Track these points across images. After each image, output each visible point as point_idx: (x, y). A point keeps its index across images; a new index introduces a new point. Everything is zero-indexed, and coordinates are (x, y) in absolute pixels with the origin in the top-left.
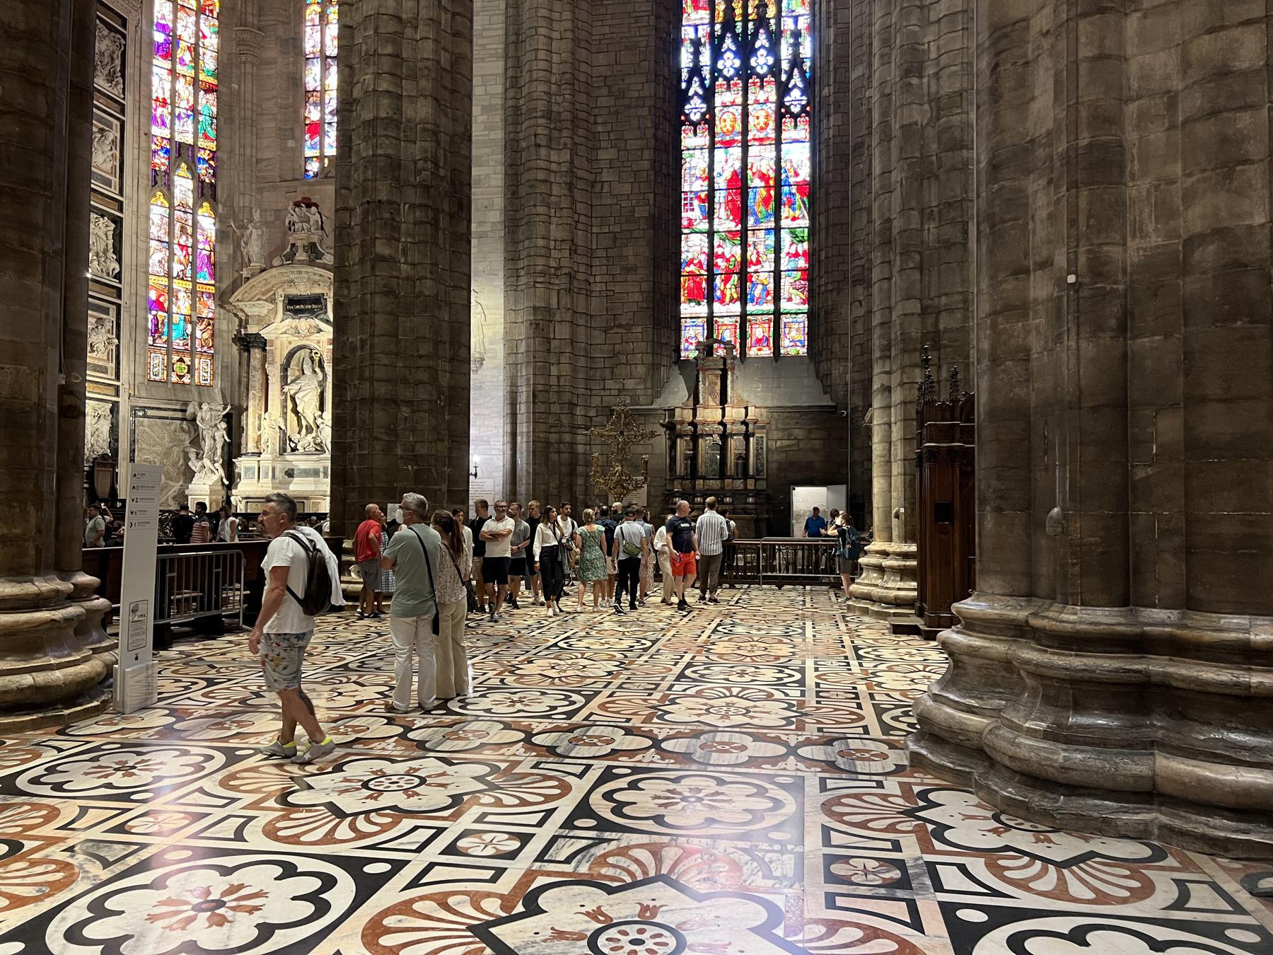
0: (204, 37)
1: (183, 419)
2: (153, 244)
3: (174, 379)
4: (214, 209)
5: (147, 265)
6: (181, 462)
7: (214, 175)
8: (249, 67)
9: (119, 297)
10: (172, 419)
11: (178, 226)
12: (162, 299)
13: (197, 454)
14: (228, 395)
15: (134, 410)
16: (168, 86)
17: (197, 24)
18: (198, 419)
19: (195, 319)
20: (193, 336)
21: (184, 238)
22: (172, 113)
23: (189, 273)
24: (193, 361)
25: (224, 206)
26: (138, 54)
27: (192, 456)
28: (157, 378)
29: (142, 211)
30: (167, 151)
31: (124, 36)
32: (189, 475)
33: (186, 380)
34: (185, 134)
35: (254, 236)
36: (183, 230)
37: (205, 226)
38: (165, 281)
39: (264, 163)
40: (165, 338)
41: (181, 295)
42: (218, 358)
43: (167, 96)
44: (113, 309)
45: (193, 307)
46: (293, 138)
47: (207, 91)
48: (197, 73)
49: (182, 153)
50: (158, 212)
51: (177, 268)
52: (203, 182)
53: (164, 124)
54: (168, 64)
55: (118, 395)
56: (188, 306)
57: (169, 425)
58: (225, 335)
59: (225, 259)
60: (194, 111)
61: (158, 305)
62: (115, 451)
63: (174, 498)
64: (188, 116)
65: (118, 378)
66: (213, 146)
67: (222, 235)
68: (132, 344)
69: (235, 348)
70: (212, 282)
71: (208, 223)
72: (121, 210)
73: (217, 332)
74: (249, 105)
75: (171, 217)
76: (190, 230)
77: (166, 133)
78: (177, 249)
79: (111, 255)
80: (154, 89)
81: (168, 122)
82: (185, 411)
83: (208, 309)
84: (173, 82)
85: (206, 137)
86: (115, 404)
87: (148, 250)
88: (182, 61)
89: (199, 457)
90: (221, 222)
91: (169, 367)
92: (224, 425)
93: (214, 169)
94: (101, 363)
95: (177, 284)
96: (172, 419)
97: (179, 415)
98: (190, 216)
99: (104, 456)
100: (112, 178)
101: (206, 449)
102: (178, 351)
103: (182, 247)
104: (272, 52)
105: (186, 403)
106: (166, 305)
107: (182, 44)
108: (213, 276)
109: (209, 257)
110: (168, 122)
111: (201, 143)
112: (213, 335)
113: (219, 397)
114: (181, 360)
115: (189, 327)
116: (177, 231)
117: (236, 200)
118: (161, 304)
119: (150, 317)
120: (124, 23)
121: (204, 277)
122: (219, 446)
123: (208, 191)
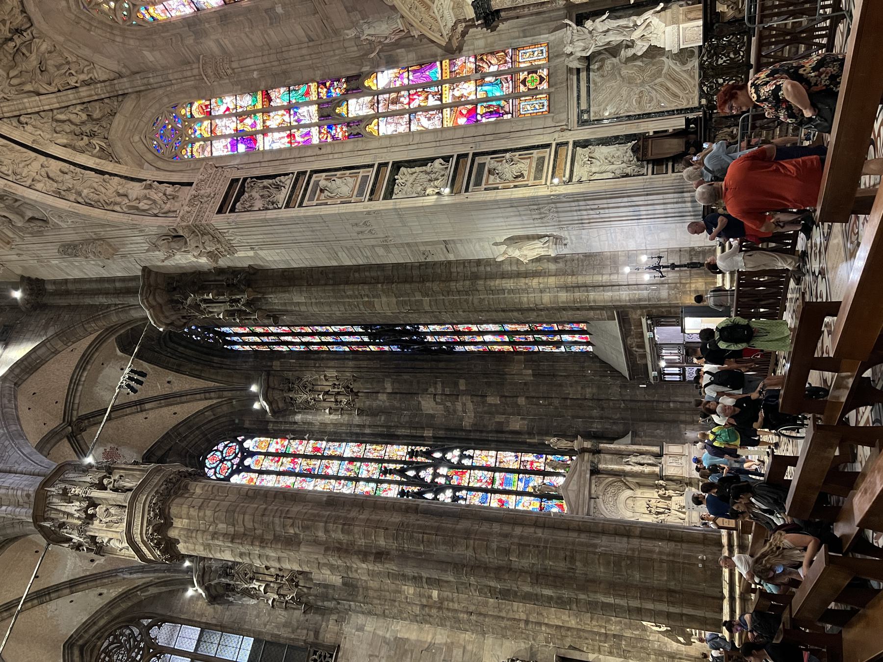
0: (228, 109)
1: (588, 70)
2: (414, 128)
3: (545, 85)
4: (368, 75)
5: (435, 131)
6: (639, 63)
7: (339, 80)
8: (235, 65)
9: (467, 155)
10: (588, 81)
11: (392, 107)
12: (464, 112)
13: (628, 47)
14: (553, 25)
15: (582, 123)
16: (277, 135)
17: (220, 117)
18: (584, 54)
19: (478, 76)
20: (495, 74)
21: (402, 99)
22: (298, 128)
23: (434, 89)
24: (523, 70)
25: (362, 65)
26: (258, 165)
27: (630, 52)
28: (546, 103)
29: (386, 143)
30: (330, 127)
31: (245, 179)
32: (654, 52)
33: (544, 73)
34: (309, 114)
35: (372, 31)
36: (395, 102)
37: (387, 81)
38: (447, 111)
39: (310, 33)
40: (502, 103)
41: (457, 93)
42: (515, 43)
43: (284, 134)
44: (479, 160)
45: (467, 79)
46: (273, 9)
47: (270, 100)
48: (258, 111)
49: (328, 113)
50: (385, 128)
51: (432, 102)
52: (347, 90)
53: (308, 134)
54: (260, 137)
55: (567, 143)
56: (466, 85)
57: (595, 84)
58: (490, 40)
59: (412, 56)
60: (289, 108)
61: (472, 114)
62: (629, 138)
63: (684, 64)
64: (295, 113)
65: (548, 146)
66: (313, 86)
67: (391, 63)
68: (512, 135)
69: (502, 26)
70: (438, 64)
71: (384, 79)
72: (386, 164)
73: (488, 50)
74: (265, 59)
75: (386, 115)
76: (393, 95)
77: (314, 131)
78: (414, 105)
79: (428, 168)
80: (283, 146)
81: (305, 131)
82: (578, 70)
83: (466, 63)
84: (272, 130)
85: (307, 93)
86: (576, 144)
87: (420, 133)
88: (254, 125)
89: (631, 45)
90: (378, 66)
91: (533, 93)
92: (589, 24)
93: (333, 82)
94: (534, 165)
95: (448, 99)
96: (588, 81)
97: (583, 75)
98: (381, 97)
99: (635, 150)
100: (361, 175)
101: (620, 38)
102: (514, 88)
103: (412, 100)
104: (210, 44)
105: (570, 70)
106: (470, 107)
107: (240, 127)
108: (432, 65)
109: (415, 72)
110: (305, 131)
111: (314, 97)
112: (492, 53)
113: (559, 34)
114: (524, 82)
115: (487, 79)
116: (397, 107)
117: (353, 55)
118: (469, 111)
119: (484, 120)
120: (234, 181)
121: (435, 73)
122: (614, 23)
123: (354, 84)
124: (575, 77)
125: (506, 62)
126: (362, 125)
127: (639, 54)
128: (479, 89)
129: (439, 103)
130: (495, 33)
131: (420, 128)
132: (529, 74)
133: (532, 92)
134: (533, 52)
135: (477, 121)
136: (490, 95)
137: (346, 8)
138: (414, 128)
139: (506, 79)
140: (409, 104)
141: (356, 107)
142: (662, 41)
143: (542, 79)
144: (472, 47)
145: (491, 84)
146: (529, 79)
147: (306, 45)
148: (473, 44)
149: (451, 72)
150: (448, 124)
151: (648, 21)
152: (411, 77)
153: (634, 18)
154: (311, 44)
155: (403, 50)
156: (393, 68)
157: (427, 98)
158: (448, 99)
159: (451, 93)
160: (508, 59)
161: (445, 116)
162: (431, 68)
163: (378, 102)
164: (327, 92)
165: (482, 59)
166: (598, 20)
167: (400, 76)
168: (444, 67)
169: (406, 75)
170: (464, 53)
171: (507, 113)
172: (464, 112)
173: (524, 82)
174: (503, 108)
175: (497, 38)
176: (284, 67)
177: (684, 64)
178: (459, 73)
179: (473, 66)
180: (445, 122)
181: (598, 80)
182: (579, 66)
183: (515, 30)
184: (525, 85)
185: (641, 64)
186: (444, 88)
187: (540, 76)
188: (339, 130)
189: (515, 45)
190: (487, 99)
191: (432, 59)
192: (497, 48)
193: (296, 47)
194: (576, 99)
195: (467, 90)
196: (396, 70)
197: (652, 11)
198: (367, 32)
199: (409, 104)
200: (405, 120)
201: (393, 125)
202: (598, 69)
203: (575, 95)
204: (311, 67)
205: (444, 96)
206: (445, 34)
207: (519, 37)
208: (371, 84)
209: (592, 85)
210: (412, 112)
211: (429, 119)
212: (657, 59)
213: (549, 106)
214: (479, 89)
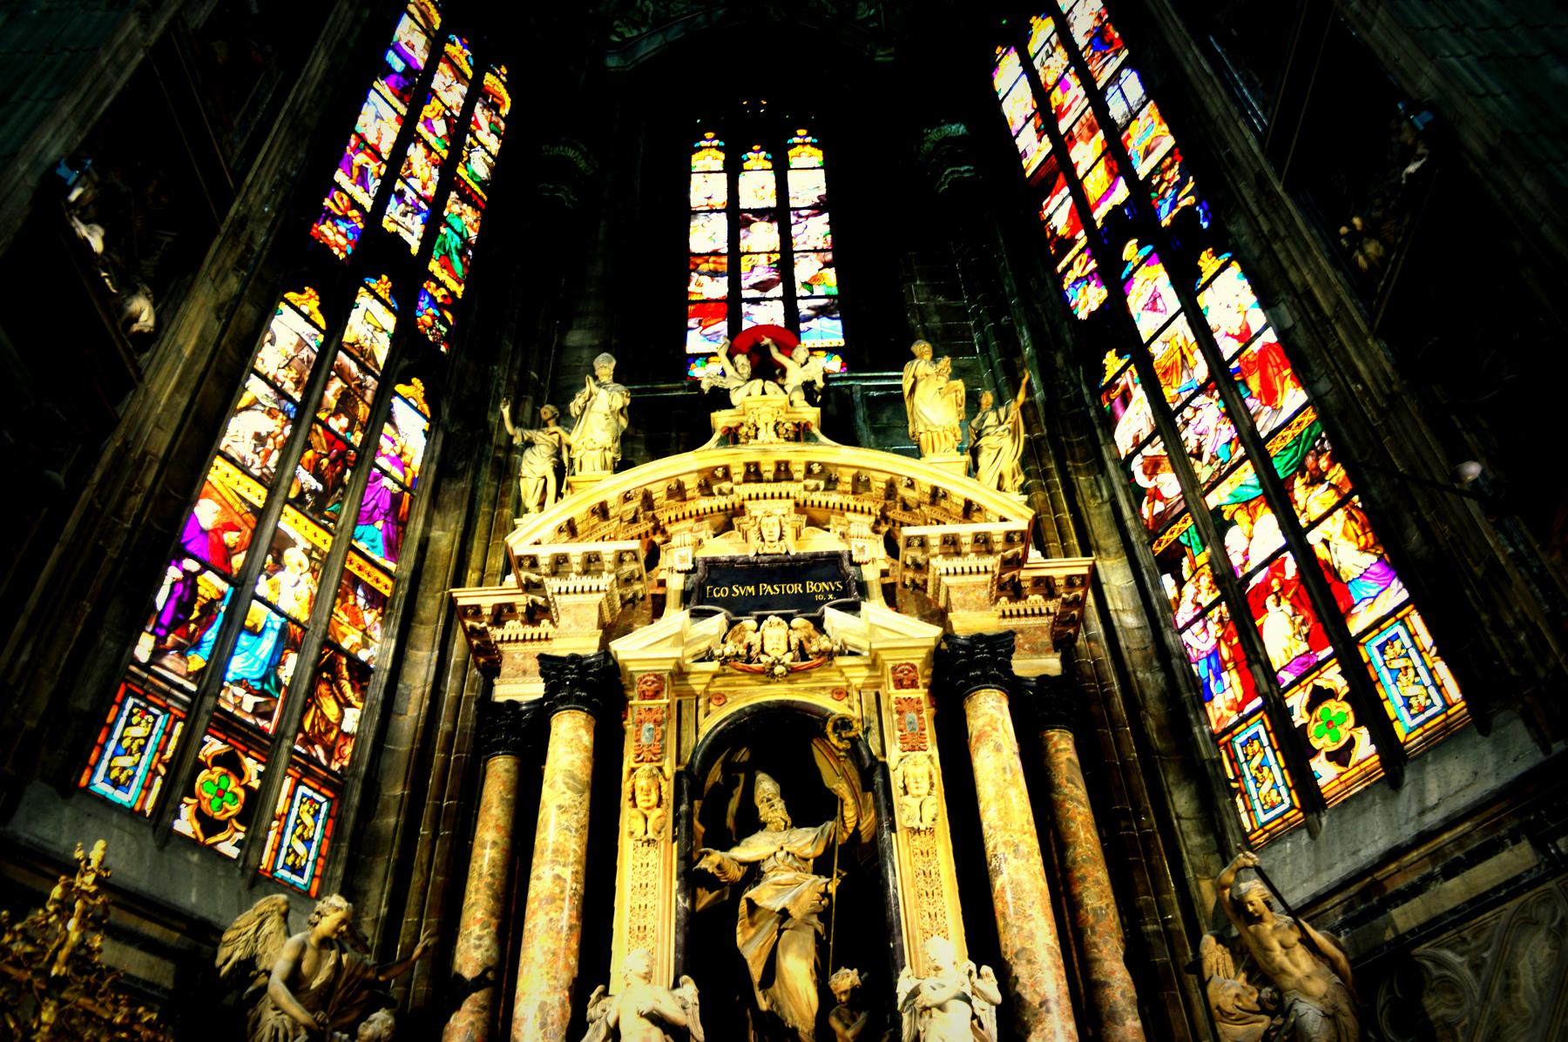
2: (255, 388)
11: (336, 385)
12: (230, 538)
28: (119, 796)
38: (257, 495)
40: (197, 661)
76: (363, 411)
102: (227, 725)
106: (237, 561)
114: (230, 763)
128: (277, 621)
132: (247, 788)
133: (189, 764)
134: (308, 842)
136: (244, 640)
139: (268, 716)
141: (371, 322)
143: (211, 825)
145: (276, 662)
146: (232, 784)
157: (317, 474)
158: (292, 523)
163: (363, 368)
164: (433, 298)
167: (397, 460)
169: (400, 477)
174: (182, 650)
184: (218, 760)
186: (322, 534)
188: (342, 241)
190: (235, 624)
211: (260, 439)
214: (277, 621)
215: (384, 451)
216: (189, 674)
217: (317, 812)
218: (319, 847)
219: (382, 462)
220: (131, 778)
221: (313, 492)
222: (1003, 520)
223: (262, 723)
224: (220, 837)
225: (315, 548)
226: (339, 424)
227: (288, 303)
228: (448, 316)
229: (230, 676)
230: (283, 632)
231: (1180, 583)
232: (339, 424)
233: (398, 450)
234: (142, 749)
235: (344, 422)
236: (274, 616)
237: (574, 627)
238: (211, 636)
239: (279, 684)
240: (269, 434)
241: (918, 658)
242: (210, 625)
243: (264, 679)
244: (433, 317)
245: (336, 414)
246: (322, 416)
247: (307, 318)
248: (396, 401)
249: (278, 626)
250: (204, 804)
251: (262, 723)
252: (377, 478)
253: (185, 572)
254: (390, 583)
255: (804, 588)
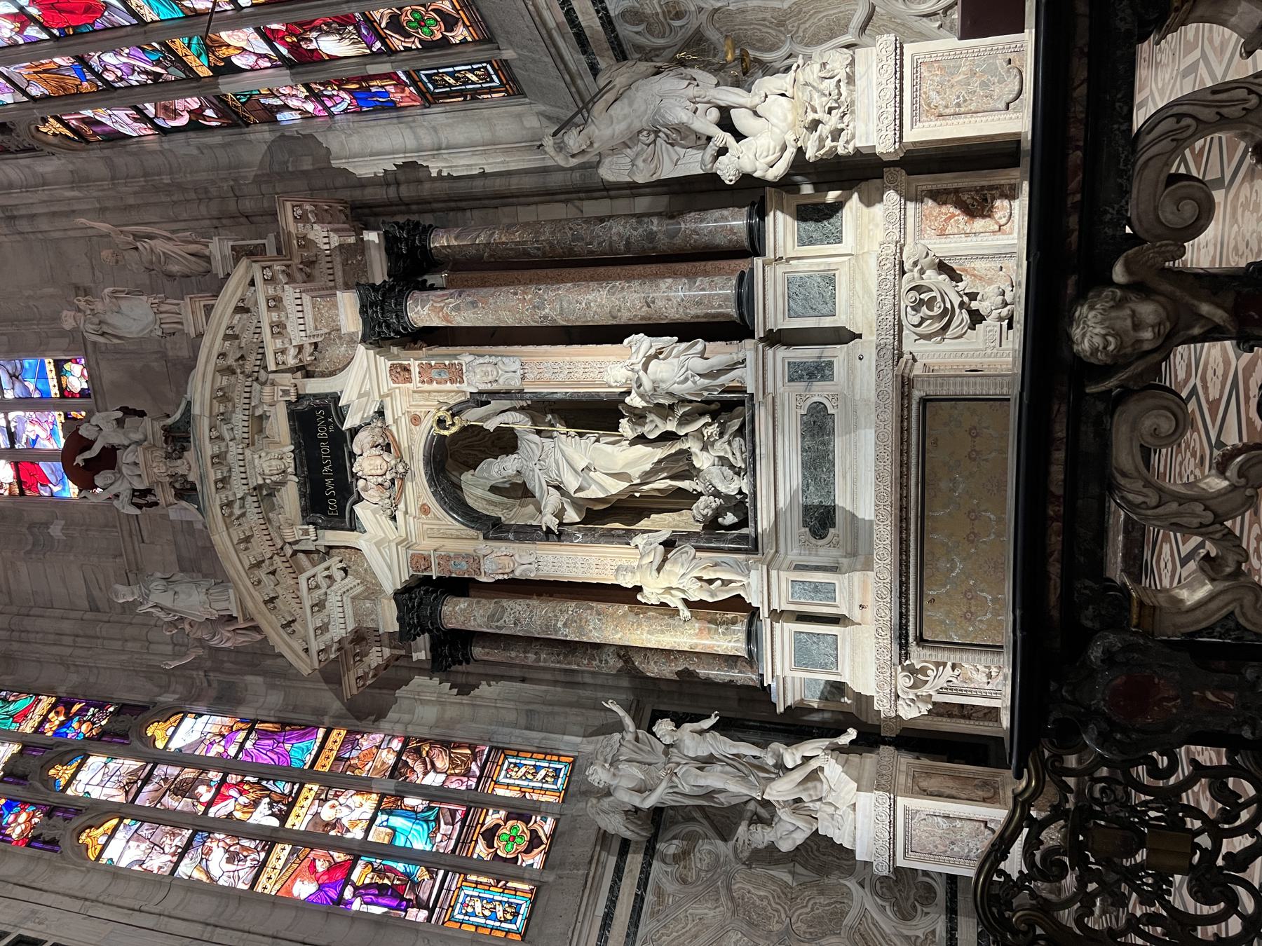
1: (650, 852)
2: (186, 869)
3: (536, 860)
6: (783, 875)
7: (101, 706)
10: (643, 883)
11: (170, 802)
12: (321, 866)
13: (756, 820)
18: (636, 800)
20: (434, 795)
24: (499, 803)
25: (166, 689)
27: (762, 836)
28: (524, 910)
29: (96, 885)
32: (824, 855)
35: (166, 600)
37: (196, 736)
38: (282, 852)
39: (96, 593)
40: (420, 873)
41: (327, 814)
42: (505, 736)
45: (362, 786)
50: (123, 849)
51: (262, 817)
52: (104, 732)
57: (660, 893)
58: (451, 712)
59: (275, 699)
63: (905, 915)
66: (46, 702)
67: (223, 702)
70: (321, 732)
71: (189, 733)
73: (438, 733)
75: (142, 816)
76: (189, 773)
82: (625, 845)
83: (378, 751)
89: (765, 814)
90: (197, 699)
91: (503, 870)
92: (664, 727)
93: (89, 706)
95: (299, 821)
96: (643, 883)
97: (635, 861)
102: (463, 841)
103: (219, 796)
105: (604, 838)
106: (339, 857)
108: (306, 730)
109: (264, 734)
114: (490, 835)
115: (410, 801)
119: (357, 905)
121: (301, 752)
122: (725, 746)
124: (612, 861)
125: (467, 773)
126: (77, 822)
127: (785, 846)
128: (381, 818)
129: (275, 822)
130: (465, 700)
131: (197, 875)
132: (507, 819)
133: (499, 866)
134: (537, 769)
135: (340, 900)
136: (400, 842)
137: (180, 559)
138: (185, 869)
139: (453, 813)
140: (209, 805)
141: (97, 778)
142: (848, 828)
143: (534, 841)
144: (406, 717)
145: (413, 814)
146: (505, 831)
147: (78, 615)
148: (412, 711)
149: (338, 759)
150: (268, 885)
151: (814, 764)
152: (249, 745)
153: (777, 746)
154: (89, 615)
155: (260, 679)
156: (222, 713)
157: (255, 804)
158: (299, 821)
159: (313, 810)
160: (474, 767)
161: (272, 860)
162: (301, 738)
163: (146, 781)
164: (62, 725)
165: (417, 751)
166: (688, 727)
167: (226, 737)
168: (329, 744)
169: (242, 735)
170: (384, 724)
171: (420, 905)
172: (321, 866)
173: (490, 835)
174: (416, 885)
175: (468, 711)
176: (15, 646)
177: (905, 915)
178: (355, 767)
179: (391, 759)
180: (263, 879)
181: (670, 887)
182: (627, 834)
183: (511, 705)
184: (490, 845)
185: (787, 878)
186: (305, 792)
187: (533, 832)
188: (23, 817)
189: (500, 740)
190: (388, 851)
191: (309, 718)
192: (459, 735)
193: (58, 613)
194: (598, 923)
195: (353, 812)
196: (227, 721)
197: (826, 742)
198: (155, 598)
199: (209, 805)
200: (177, 841)
201: (144, 846)
202: (677, 858)
203: (601, 910)
204: (62, 662)
205: (296, 810)
206: (315, 646)
207: (515, 725)
208: (159, 734)
209: (650, 897)
210: (202, 827)
211: (232, 858)
212: (832, 880)
213: (529, 919)
214: (381, 818)
215: (221, 750)
216: (431, 878)
217: (515, 765)
218: (539, 760)
219: (232, 751)
220: (510, 905)
221: (271, 805)
222: (252, 283)
223: (458, 817)
224: (541, 833)
225: (317, 797)
226: (205, 794)
227: (99, 857)
228: (76, 707)
229: (428, 848)
230: (390, 812)
231: (286, 107)
232: (205, 794)
233: (218, 739)
234: (490, 901)
235: (202, 789)
236: (378, 821)
237: (373, 616)
238: (400, 867)
239: (429, 808)
240: (227, 851)
241: (384, 364)
242: (392, 870)
243: (427, 821)
244: (81, 722)
245: (196, 798)
246: (201, 808)
247: (111, 837)
248: (173, 746)
249: (385, 817)
250: (521, 849)
251: (458, 817)
252: (248, 754)
253: (355, 896)
254: (335, 732)
255: (324, 440)
